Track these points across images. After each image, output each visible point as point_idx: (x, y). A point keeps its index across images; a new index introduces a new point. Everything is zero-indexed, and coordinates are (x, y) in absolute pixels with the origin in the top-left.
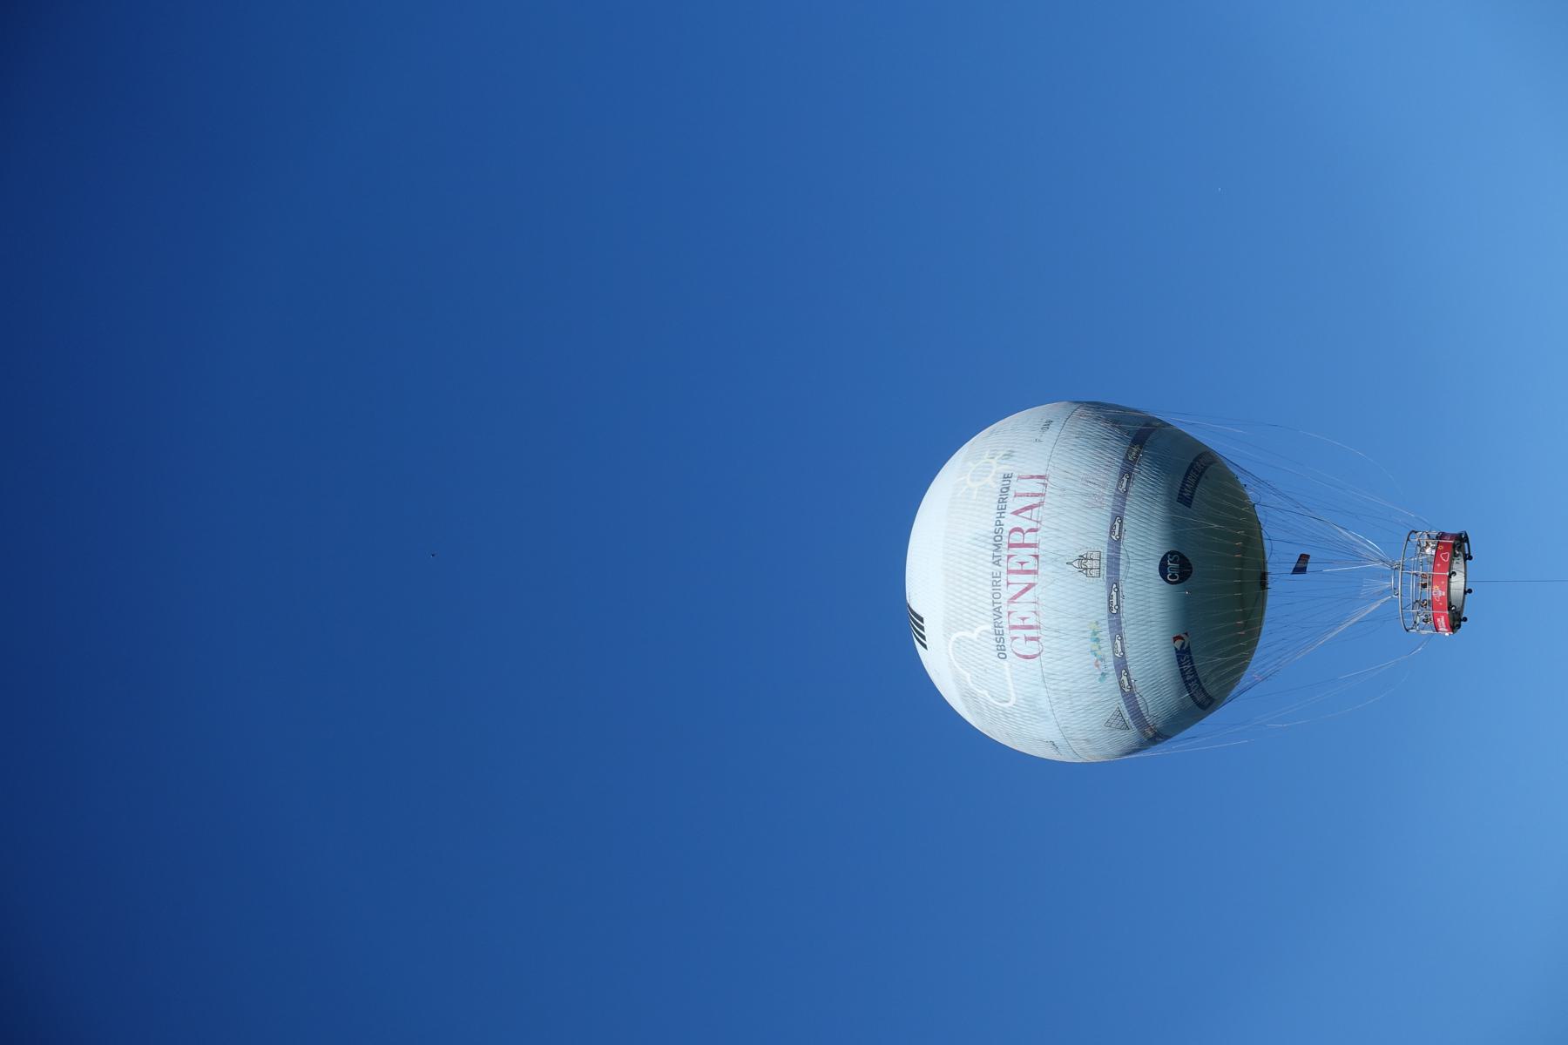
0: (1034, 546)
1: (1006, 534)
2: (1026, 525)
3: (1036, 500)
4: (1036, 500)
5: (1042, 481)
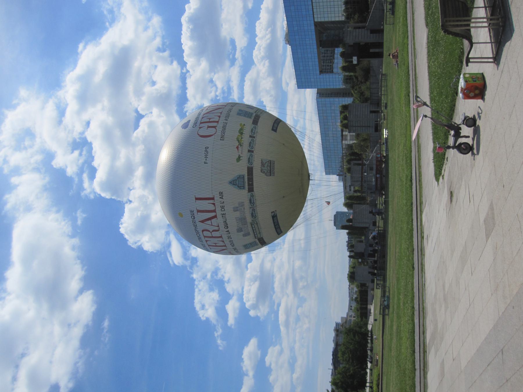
0: (221, 237)
1: (201, 233)
2: (211, 228)
3: (213, 214)
4: (213, 214)
5: (212, 201)
